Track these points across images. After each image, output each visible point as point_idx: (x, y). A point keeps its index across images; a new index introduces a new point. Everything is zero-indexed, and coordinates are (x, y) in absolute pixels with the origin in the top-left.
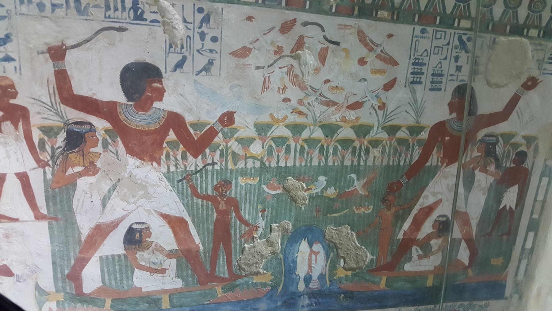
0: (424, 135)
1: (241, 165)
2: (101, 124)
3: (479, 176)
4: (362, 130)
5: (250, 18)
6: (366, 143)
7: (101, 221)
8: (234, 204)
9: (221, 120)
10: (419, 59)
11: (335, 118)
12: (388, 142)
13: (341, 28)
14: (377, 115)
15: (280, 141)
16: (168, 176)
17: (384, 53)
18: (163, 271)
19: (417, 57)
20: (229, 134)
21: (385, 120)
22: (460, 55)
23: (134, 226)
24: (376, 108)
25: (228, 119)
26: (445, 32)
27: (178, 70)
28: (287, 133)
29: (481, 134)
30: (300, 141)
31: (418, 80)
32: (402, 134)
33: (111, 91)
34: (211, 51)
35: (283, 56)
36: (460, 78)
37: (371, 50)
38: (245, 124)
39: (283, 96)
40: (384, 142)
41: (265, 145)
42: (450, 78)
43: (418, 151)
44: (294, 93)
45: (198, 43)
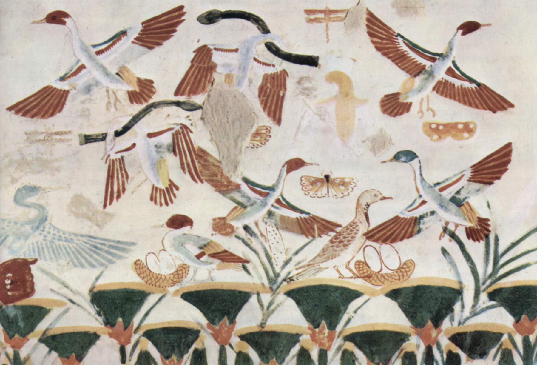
4: (427, 304)
6: (445, 342)
11: (332, 273)
12: (518, 339)
13: (316, 20)
14: (468, 258)
17: (455, 76)
20: (21, 324)
21: (496, 269)
24: (462, 234)
28: (191, 316)
30: (235, 340)
35: (154, 106)
37: (416, 71)
40: (505, 337)
41: (128, 348)
44: (202, 203)
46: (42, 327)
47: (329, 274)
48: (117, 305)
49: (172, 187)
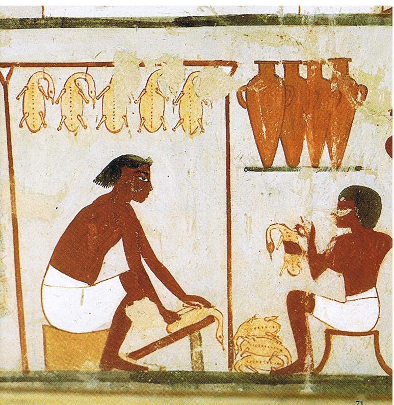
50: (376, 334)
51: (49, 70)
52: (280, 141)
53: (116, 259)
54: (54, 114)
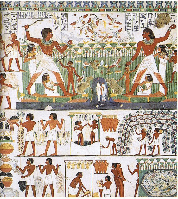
0: (136, 46)
1: (75, 57)
2: (36, 45)
3: (161, 60)
4: (114, 45)
5: (75, 15)
7: (36, 72)
8: (73, 69)
9: (68, 43)
10: (129, 22)
15: (87, 49)
16: (54, 59)
18: (53, 90)
19: (128, 22)
22: (143, 20)
23: (45, 75)
25: (70, 42)
26: (136, 13)
27: (56, 30)
28: (89, 46)
29: (158, 45)
31: (129, 29)
32: (128, 46)
33: (39, 36)
34: (65, 24)
36: (144, 27)
38: (75, 43)
39: (86, 35)
42: (141, 27)
43: (135, 51)
44: (90, 34)
45: (61, 22)
46: (73, 47)
47: (103, 42)
48: (81, 45)
49: (87, 33)
50: (110, 194)
51: (70, 161)
52: (109, 129)
53: (78, 185)
54: (71, 167)
